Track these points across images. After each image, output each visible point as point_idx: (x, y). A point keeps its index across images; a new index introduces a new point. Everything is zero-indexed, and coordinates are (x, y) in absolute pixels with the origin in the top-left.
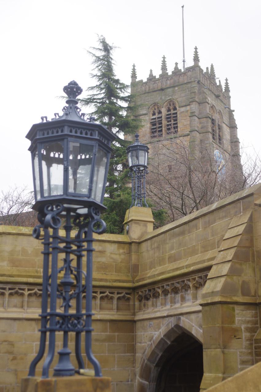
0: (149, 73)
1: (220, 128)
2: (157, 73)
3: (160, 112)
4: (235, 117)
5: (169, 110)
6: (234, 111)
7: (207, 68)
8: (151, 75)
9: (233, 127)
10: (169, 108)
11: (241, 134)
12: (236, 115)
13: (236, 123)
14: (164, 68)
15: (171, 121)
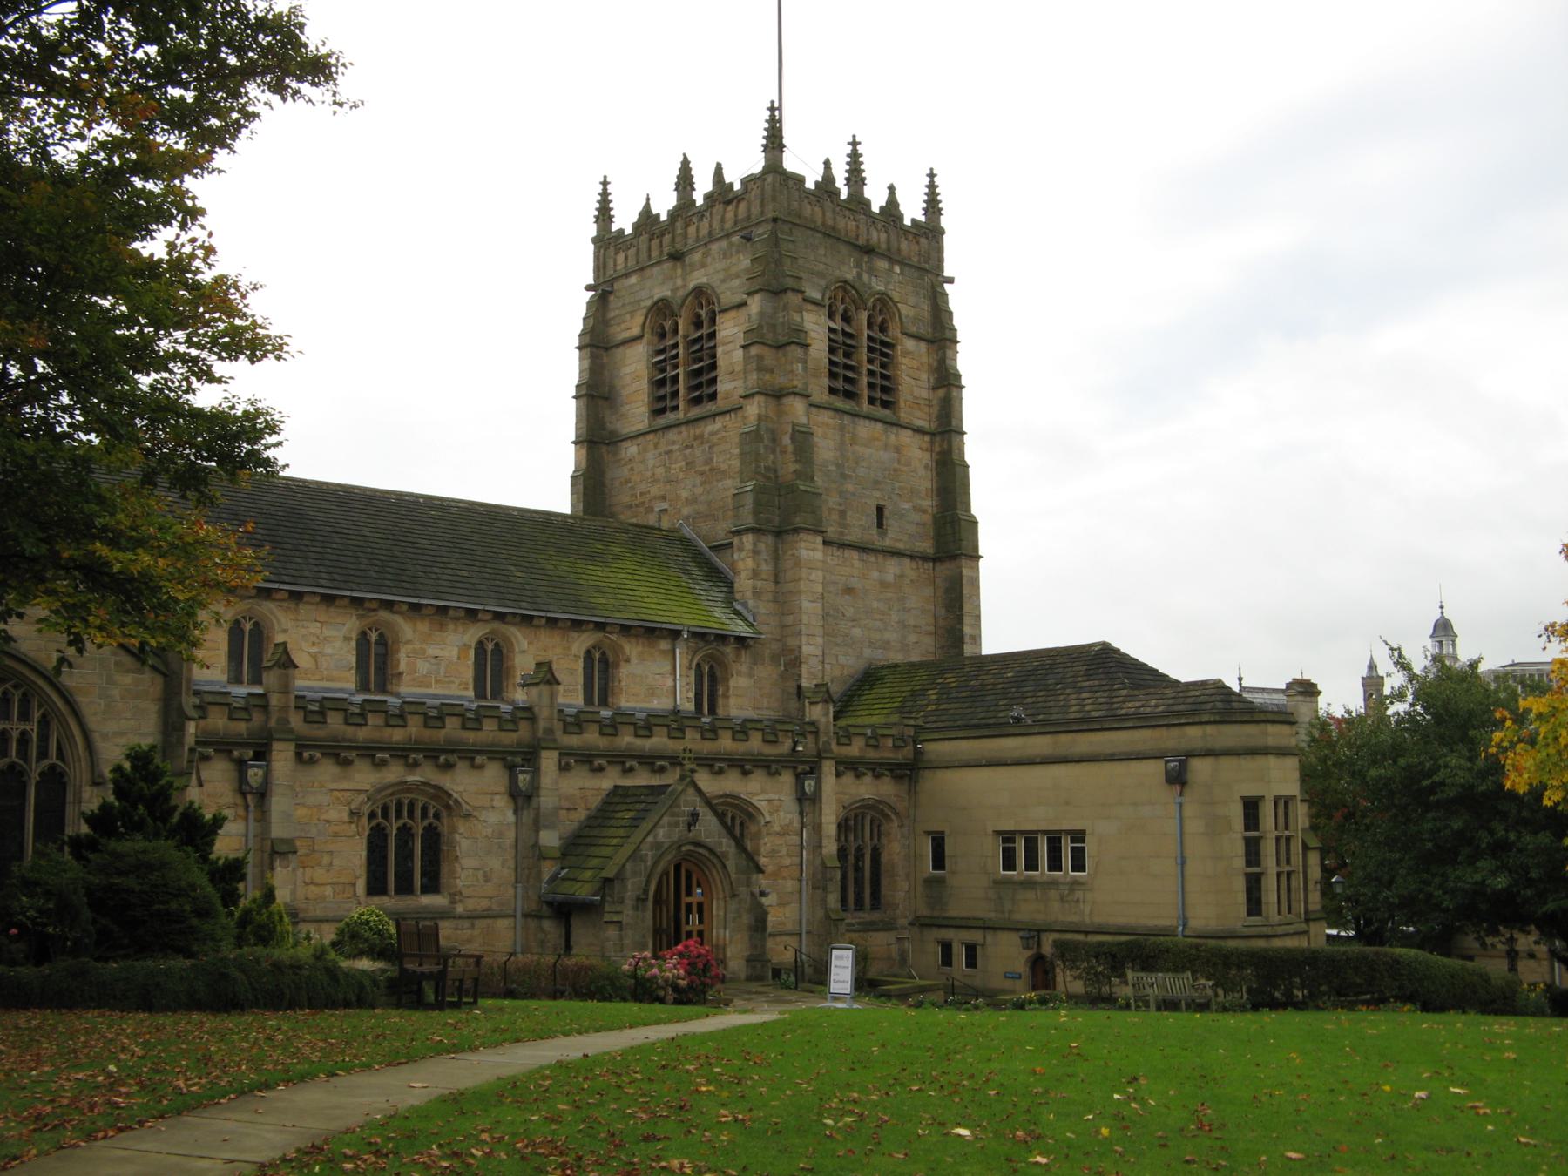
0: (645, 202)
1: (882, 350)
2: (665, 204)
3: (676, 331)
4: (954, 303)
5: (698, 324)
6: (951, 281)
7: (827, 164)
8: (647, 208)
9: (941, 335)
10: (699, 316)
11: (966, 361)
12: (956, 297)
13: (956, 323)
14: (685, 181)
15: (701, 360)
